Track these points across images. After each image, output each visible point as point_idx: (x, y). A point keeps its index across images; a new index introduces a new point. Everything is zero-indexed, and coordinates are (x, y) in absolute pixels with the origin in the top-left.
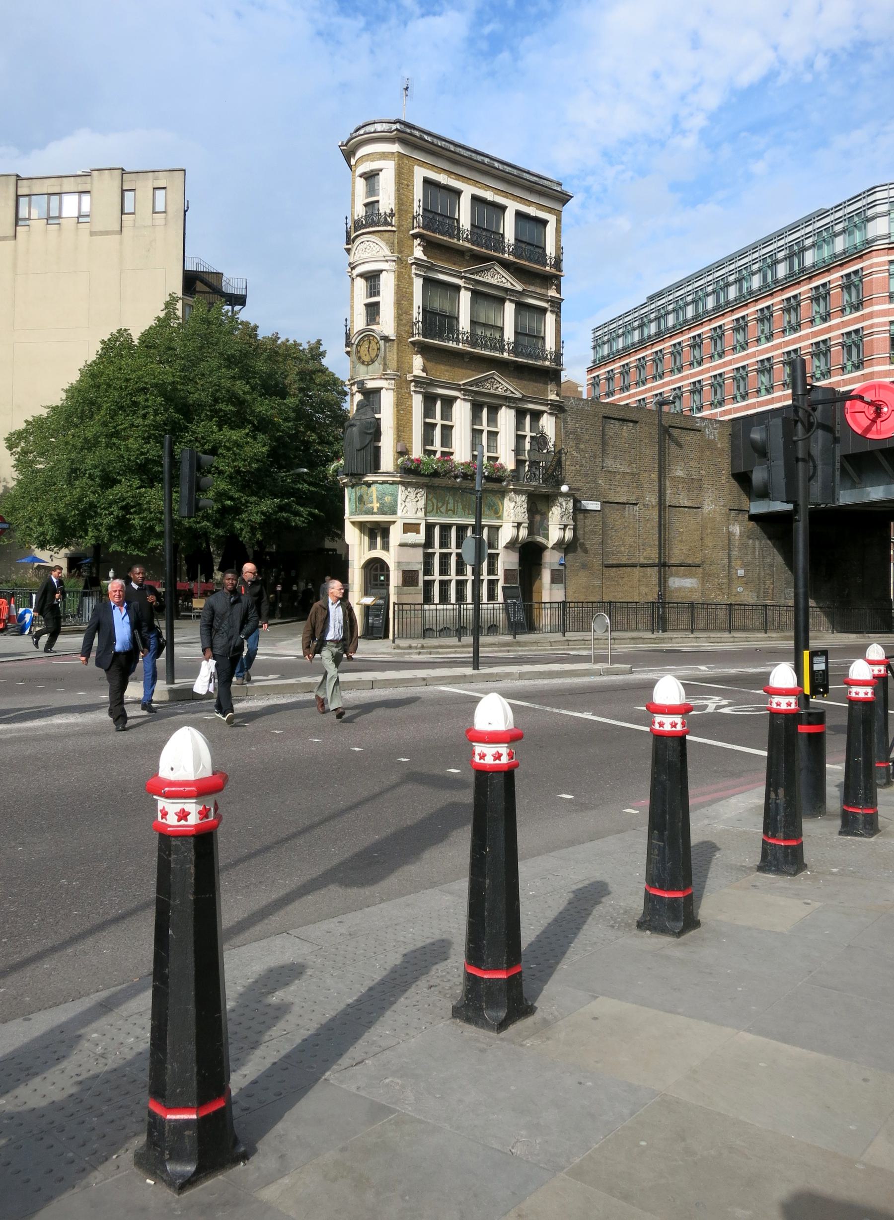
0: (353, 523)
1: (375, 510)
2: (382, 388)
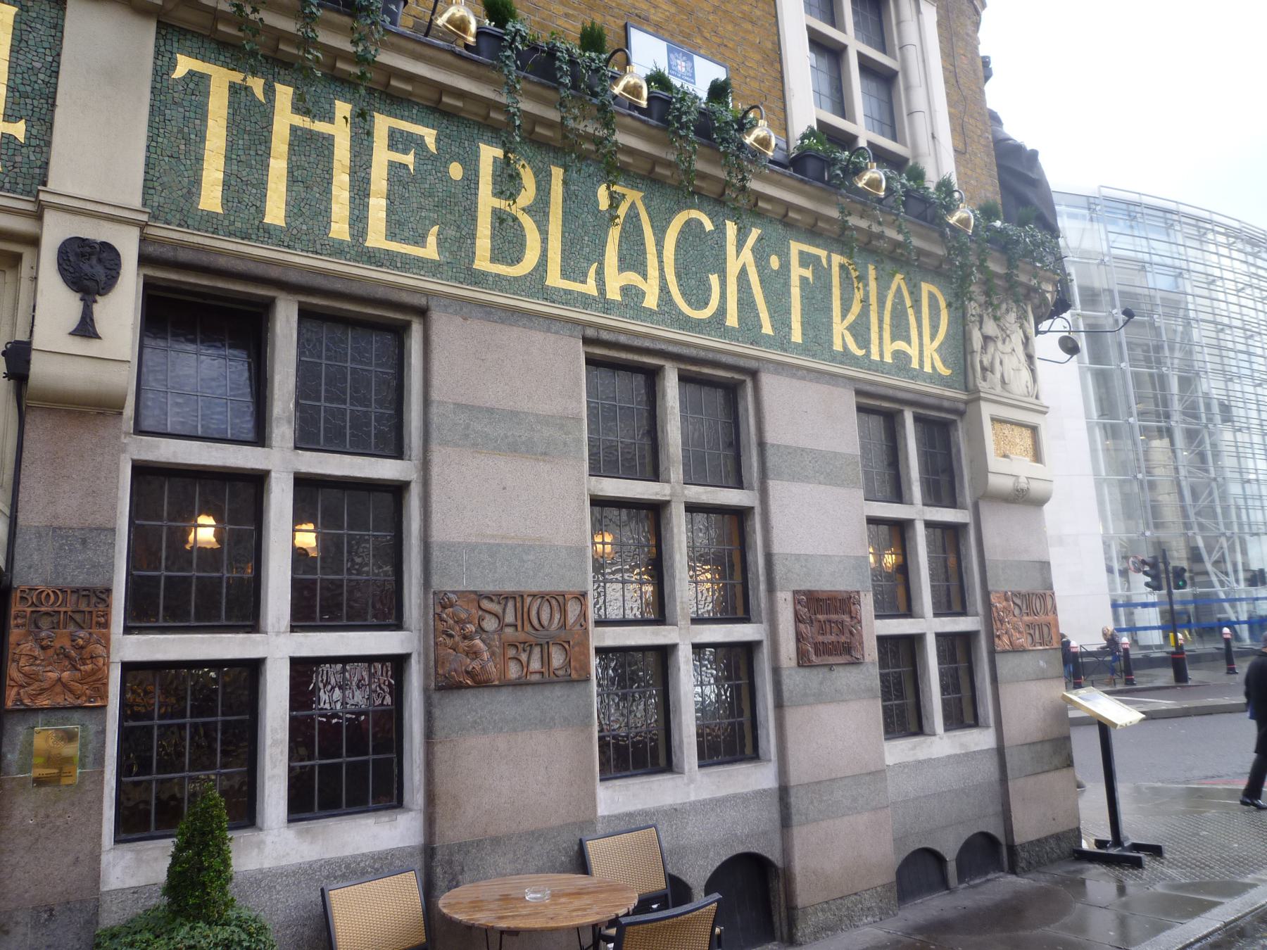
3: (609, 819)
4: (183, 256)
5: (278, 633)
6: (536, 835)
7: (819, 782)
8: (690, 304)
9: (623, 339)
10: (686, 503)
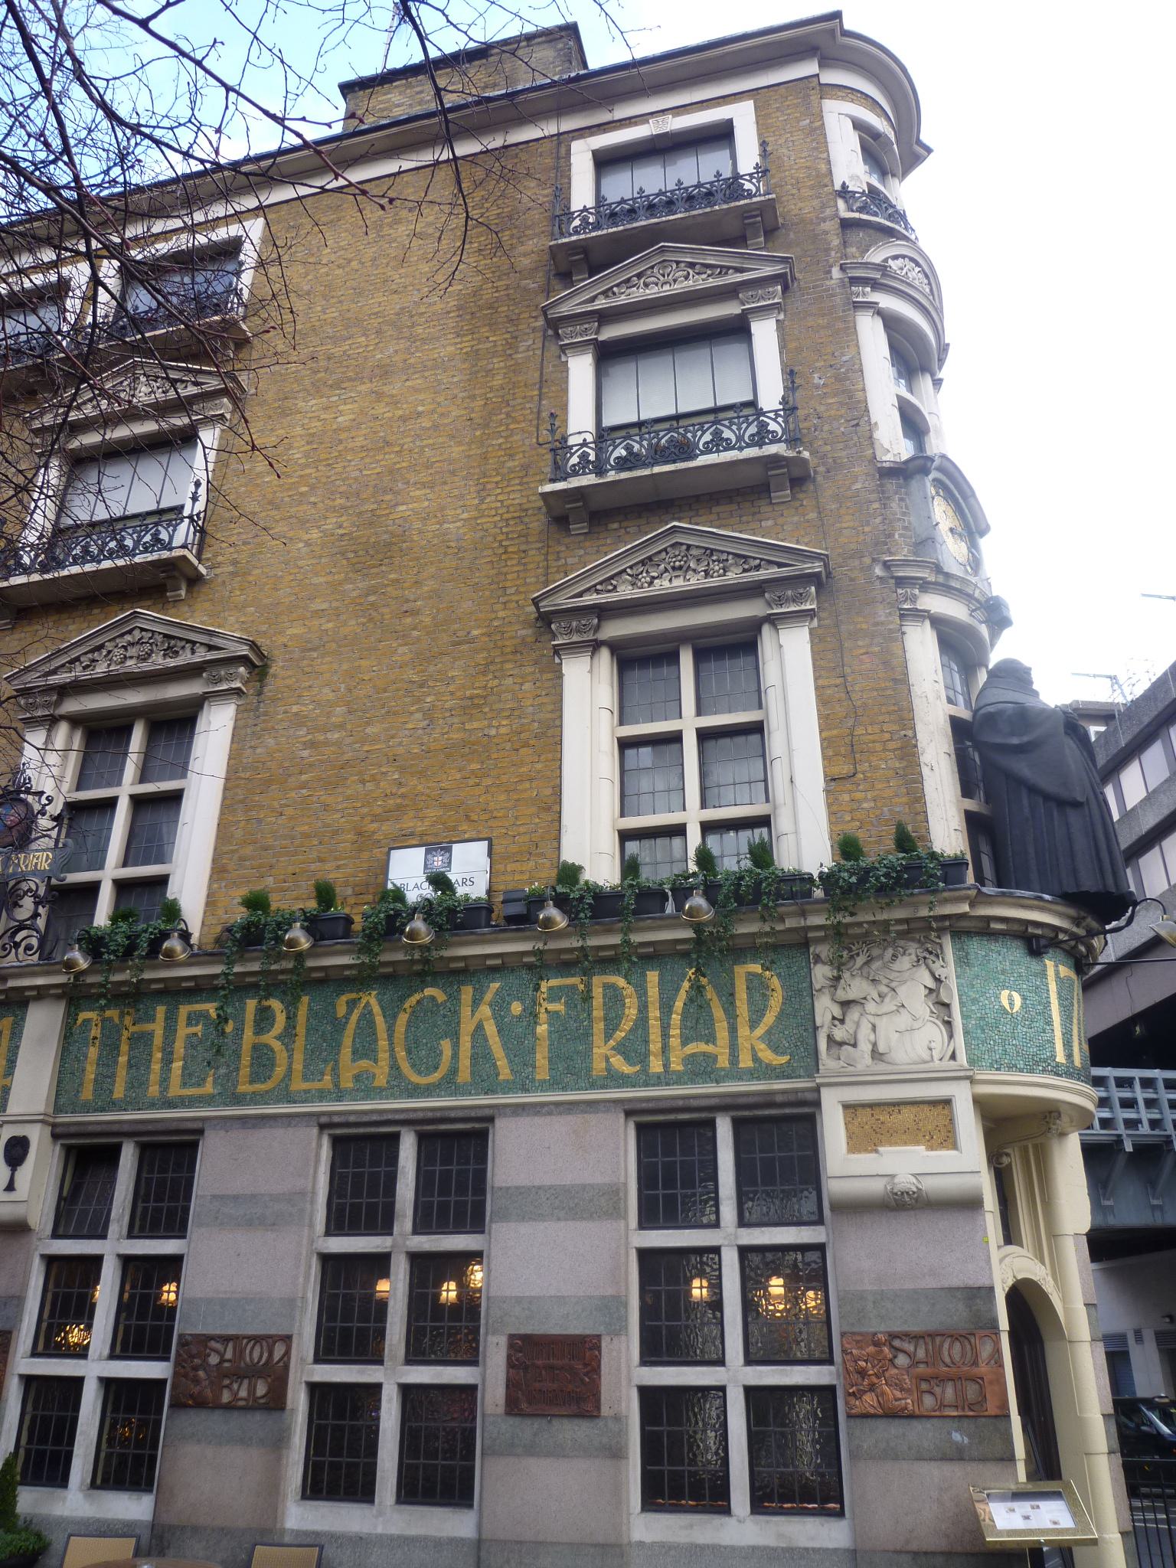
3: (298, 1533)
4: (73, 1129)
5: (93, 1360)
6: (224, 1531)
7: (521, 1542)
8: (419, 1073)
9: (352, 1119)
10: (408, 1253)
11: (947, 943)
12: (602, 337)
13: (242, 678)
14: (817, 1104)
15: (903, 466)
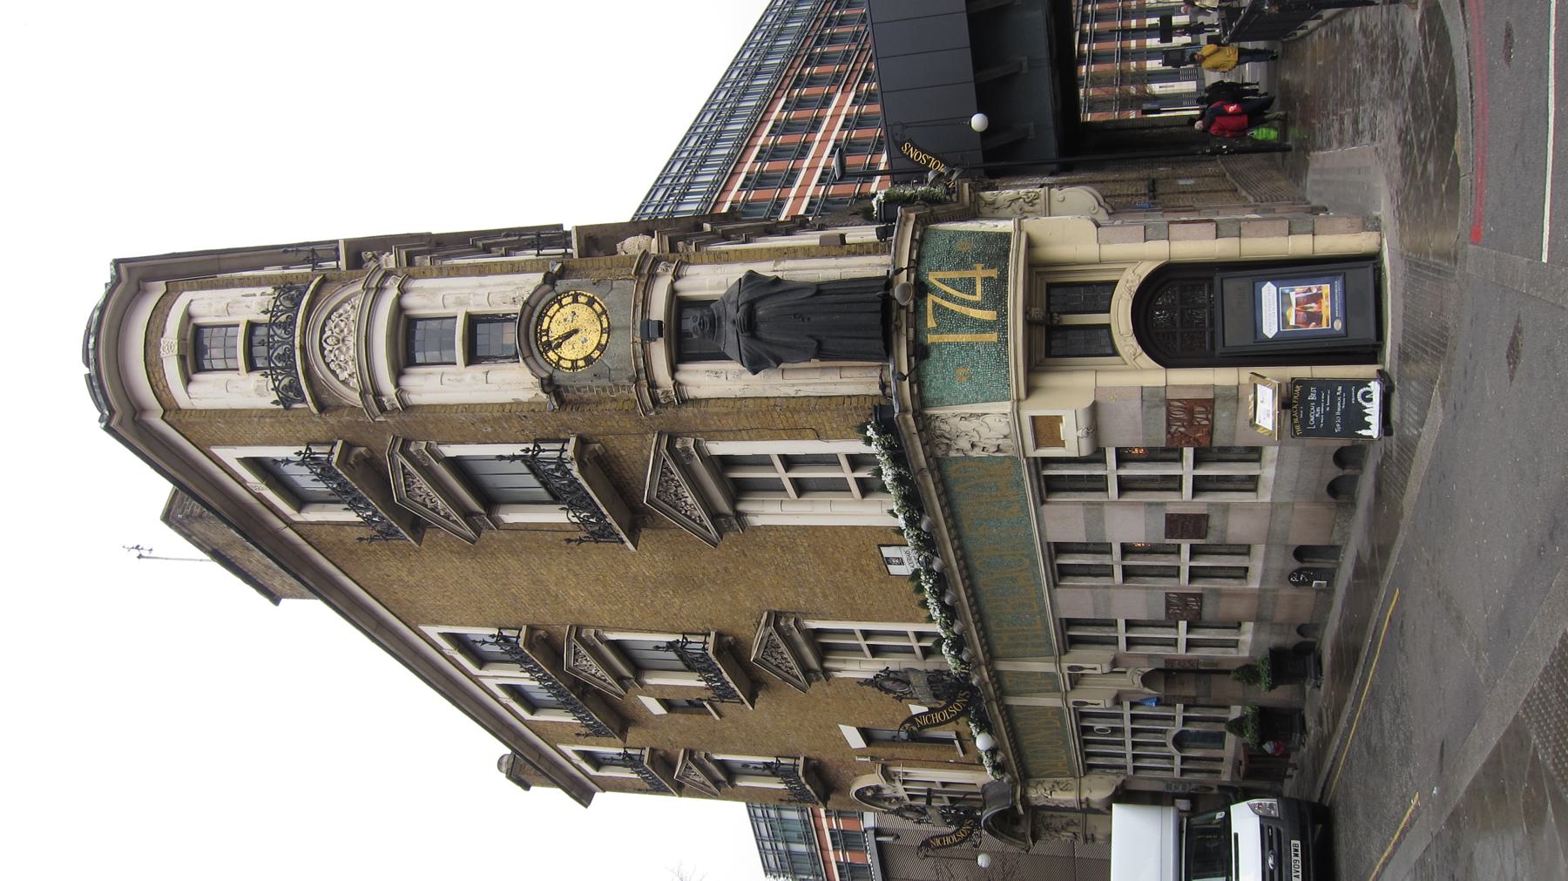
0: (1030, 390)
1: (994, 273)
2: (673, 292)
11: (930, 412)
12: (483, 511)
13: (786, 621)
14: (1035, 458)
15: (552, 393)
